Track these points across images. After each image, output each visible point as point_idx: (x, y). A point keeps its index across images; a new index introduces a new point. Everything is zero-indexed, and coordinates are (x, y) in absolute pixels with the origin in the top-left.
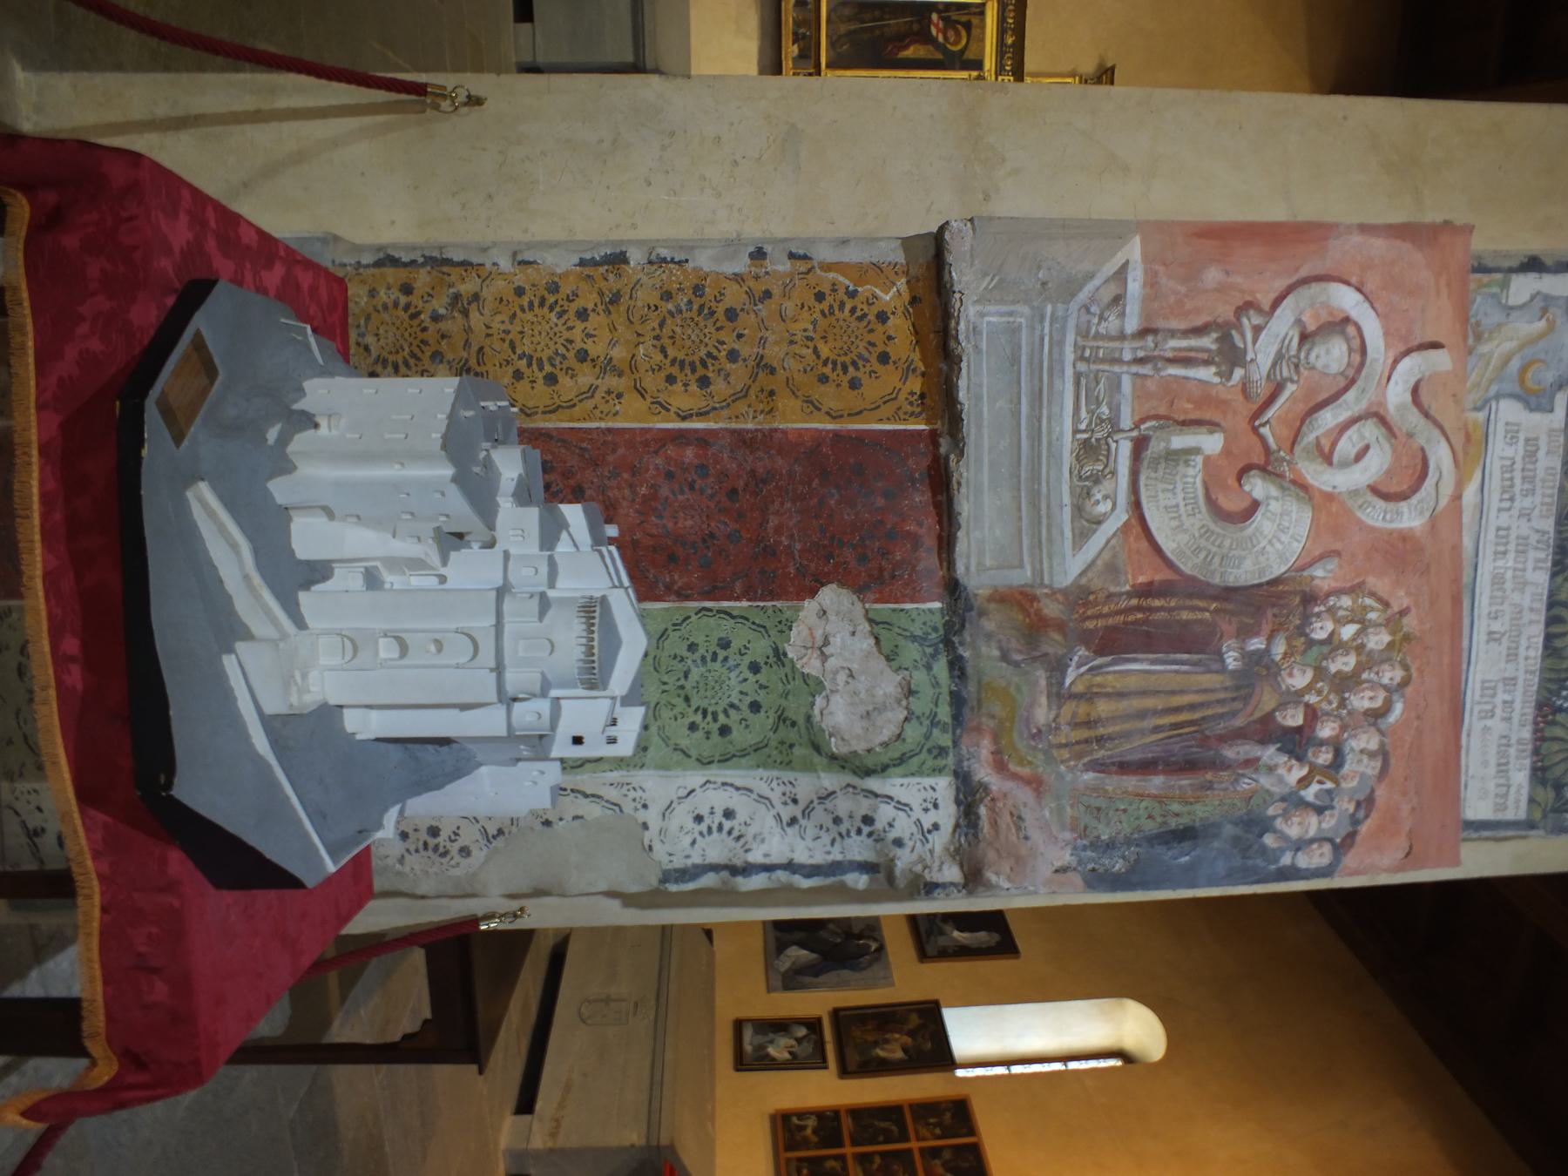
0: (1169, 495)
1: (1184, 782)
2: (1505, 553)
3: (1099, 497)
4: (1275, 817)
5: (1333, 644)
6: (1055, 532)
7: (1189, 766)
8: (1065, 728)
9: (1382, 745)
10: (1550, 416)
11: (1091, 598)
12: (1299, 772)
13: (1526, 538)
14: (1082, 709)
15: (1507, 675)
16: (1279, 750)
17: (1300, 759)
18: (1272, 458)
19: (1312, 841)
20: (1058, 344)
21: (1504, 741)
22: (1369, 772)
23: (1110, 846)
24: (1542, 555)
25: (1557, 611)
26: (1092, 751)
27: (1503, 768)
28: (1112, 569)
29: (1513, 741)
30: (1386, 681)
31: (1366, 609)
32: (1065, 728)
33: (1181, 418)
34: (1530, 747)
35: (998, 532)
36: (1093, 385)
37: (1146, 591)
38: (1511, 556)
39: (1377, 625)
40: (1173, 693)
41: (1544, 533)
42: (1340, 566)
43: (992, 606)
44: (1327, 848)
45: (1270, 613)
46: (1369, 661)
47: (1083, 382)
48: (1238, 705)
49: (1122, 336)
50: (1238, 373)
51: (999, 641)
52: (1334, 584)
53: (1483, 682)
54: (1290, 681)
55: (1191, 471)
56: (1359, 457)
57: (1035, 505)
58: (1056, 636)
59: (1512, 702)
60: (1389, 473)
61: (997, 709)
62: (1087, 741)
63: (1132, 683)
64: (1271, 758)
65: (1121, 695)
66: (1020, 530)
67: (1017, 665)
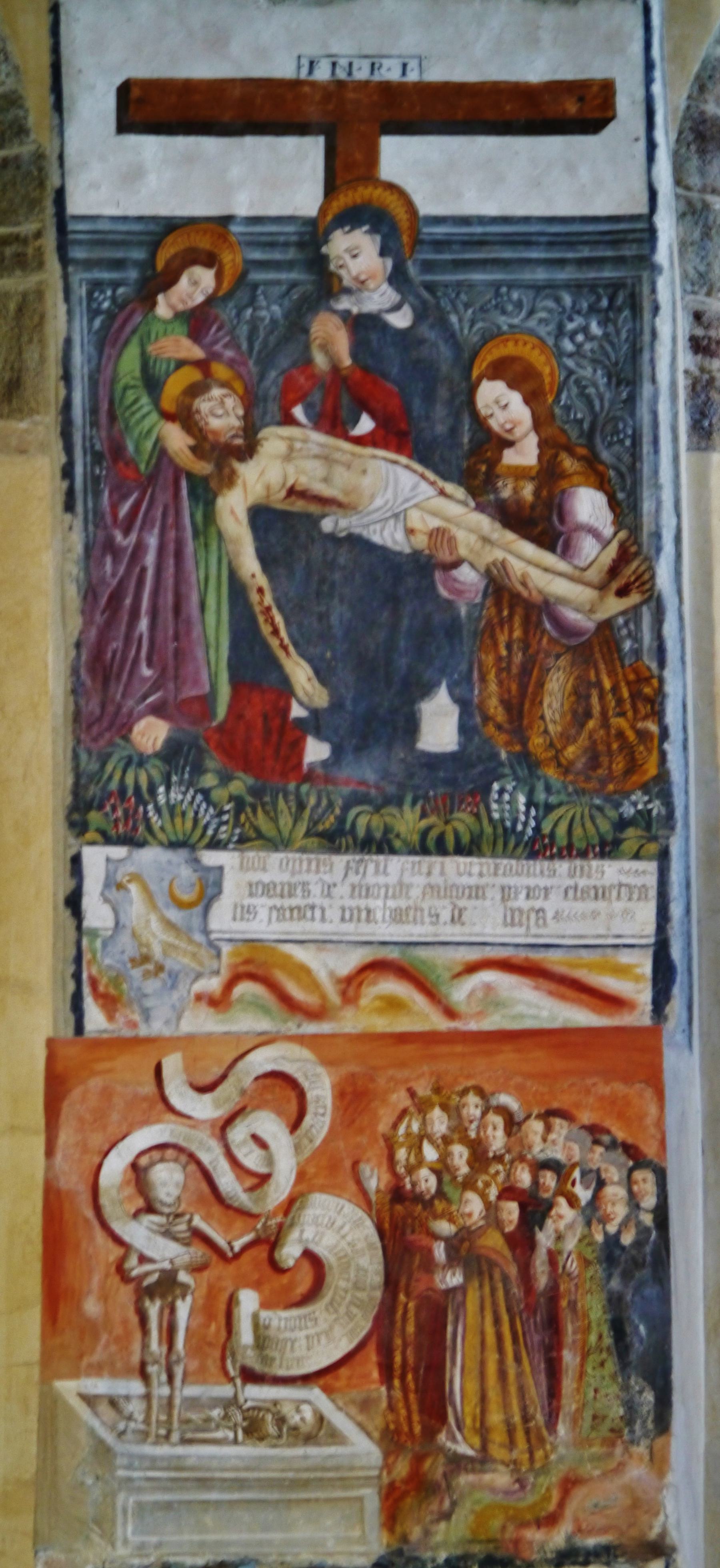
0: (297, 1345)
1: (570, 1328)
2: (369, 911)
3: (297, 1418)
4: (606, 1234)
5: (442, 1170)
6: (330, 1463)
7: (553, 1325)
8: (515, 1455)
9: (539, 1117)
10: (226, 870)
11: (392, 1427)
12: (562, 1206)
13: (353, 887)
14: (498, 1437)
15: (498, 897)
16: (541, 1229)
17: (550, 1205)
18: (263, 1236)
19: (630, 1192)
20: (153, 1463)
21: (571, 893)
22: (564, 1132)
23: (631, 1407)
24: (371, 867)
25: (431, 842)
26: (538, 1429)
27: (600, 893)
28: (365, 1405)
29: (571, 882)
30: (478, 1113)
31: (408, 1134)
32: (515, 1455)
33: (223, 1334)
34: (578, 862)
35: (329, 1523)
36: (191, 1426)
37: (387, 1372)
38: (372, 903)
39: (424, 1123)
40: (483, 1343)
41: (348, 868)
42: (368, 1161)
43: (398, 1529)
44: (638, 1175)
45: (411, 1237)
46: (458, 1132)
47: (189, 1435)
48: (497, 1276)
49: (147, 1397)
50: (183, 1277)
51: (432, 1522)
52: (385, 1167)
53: (505, 924)
54: (476, 1216)
55: (275, 1323)
56: (262, 1144)
57: (305, 1484)
58: (427, 1464)
59: (528, 888)
60: (279, 1113)
61: (496, 1524)
62: (527, 1432)
63: (473, 1387)
64: (548, 1238)
65: (483, 1399)
66: (328, 1501)
67: (454, 1504)
